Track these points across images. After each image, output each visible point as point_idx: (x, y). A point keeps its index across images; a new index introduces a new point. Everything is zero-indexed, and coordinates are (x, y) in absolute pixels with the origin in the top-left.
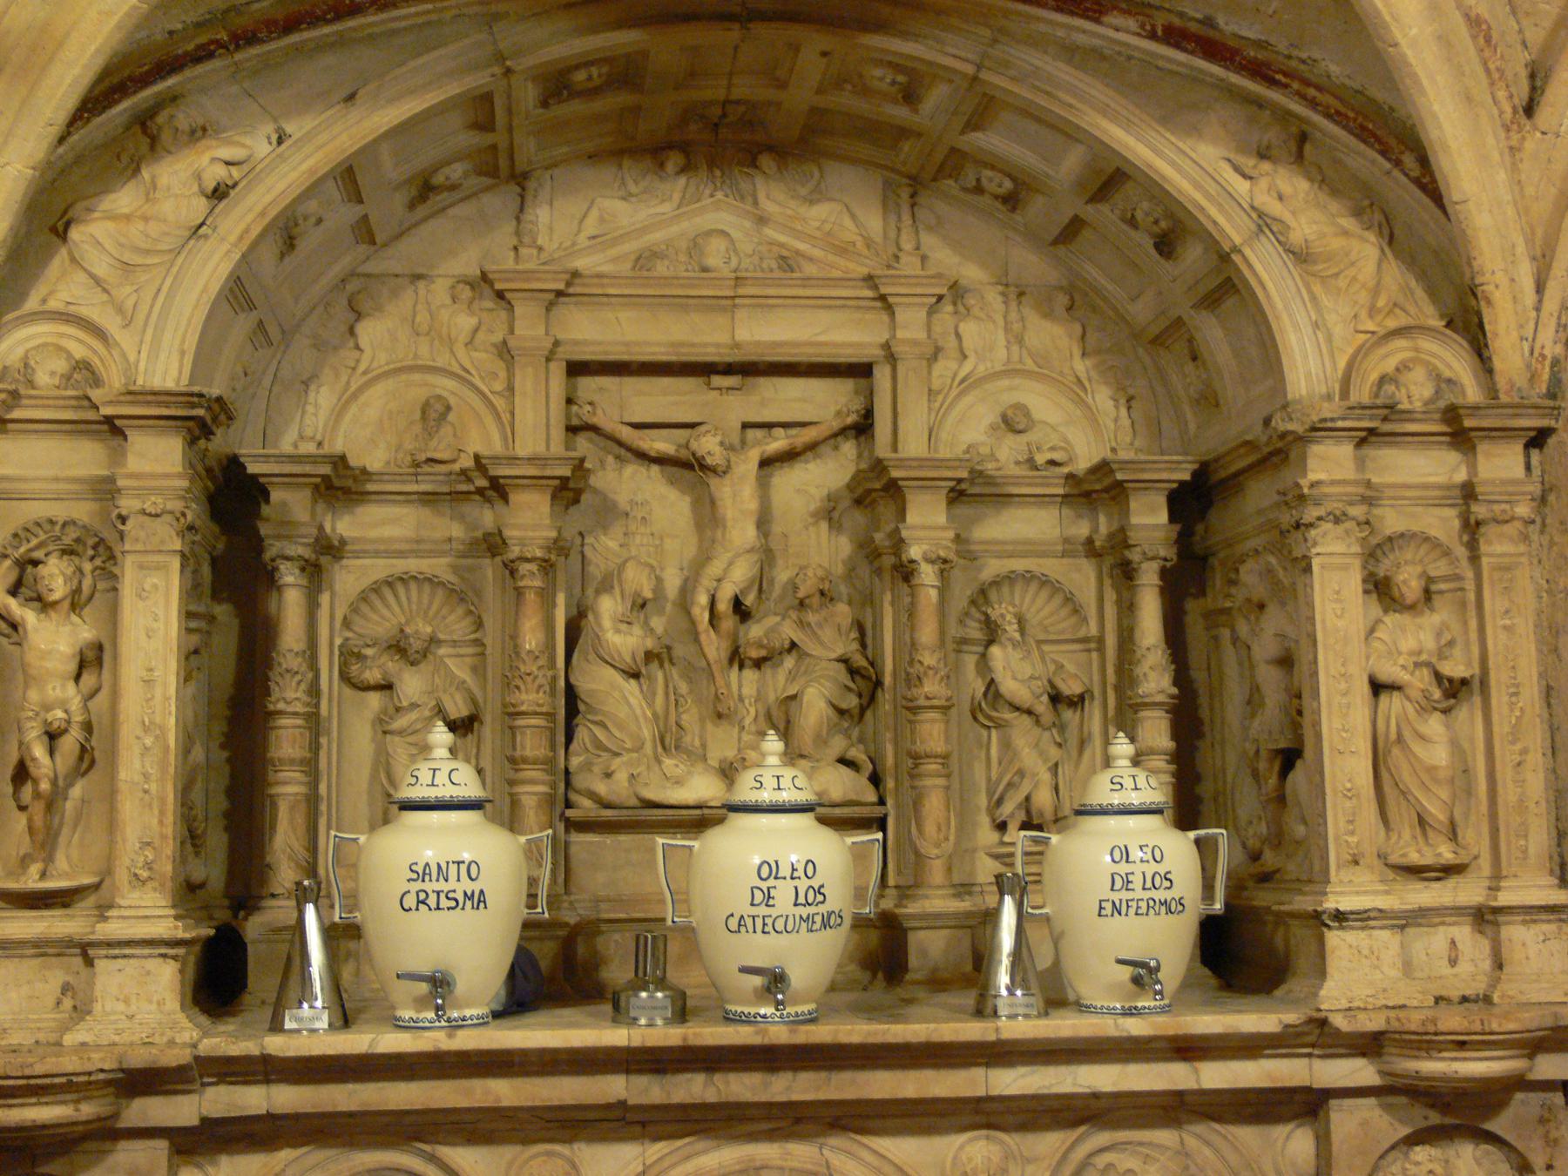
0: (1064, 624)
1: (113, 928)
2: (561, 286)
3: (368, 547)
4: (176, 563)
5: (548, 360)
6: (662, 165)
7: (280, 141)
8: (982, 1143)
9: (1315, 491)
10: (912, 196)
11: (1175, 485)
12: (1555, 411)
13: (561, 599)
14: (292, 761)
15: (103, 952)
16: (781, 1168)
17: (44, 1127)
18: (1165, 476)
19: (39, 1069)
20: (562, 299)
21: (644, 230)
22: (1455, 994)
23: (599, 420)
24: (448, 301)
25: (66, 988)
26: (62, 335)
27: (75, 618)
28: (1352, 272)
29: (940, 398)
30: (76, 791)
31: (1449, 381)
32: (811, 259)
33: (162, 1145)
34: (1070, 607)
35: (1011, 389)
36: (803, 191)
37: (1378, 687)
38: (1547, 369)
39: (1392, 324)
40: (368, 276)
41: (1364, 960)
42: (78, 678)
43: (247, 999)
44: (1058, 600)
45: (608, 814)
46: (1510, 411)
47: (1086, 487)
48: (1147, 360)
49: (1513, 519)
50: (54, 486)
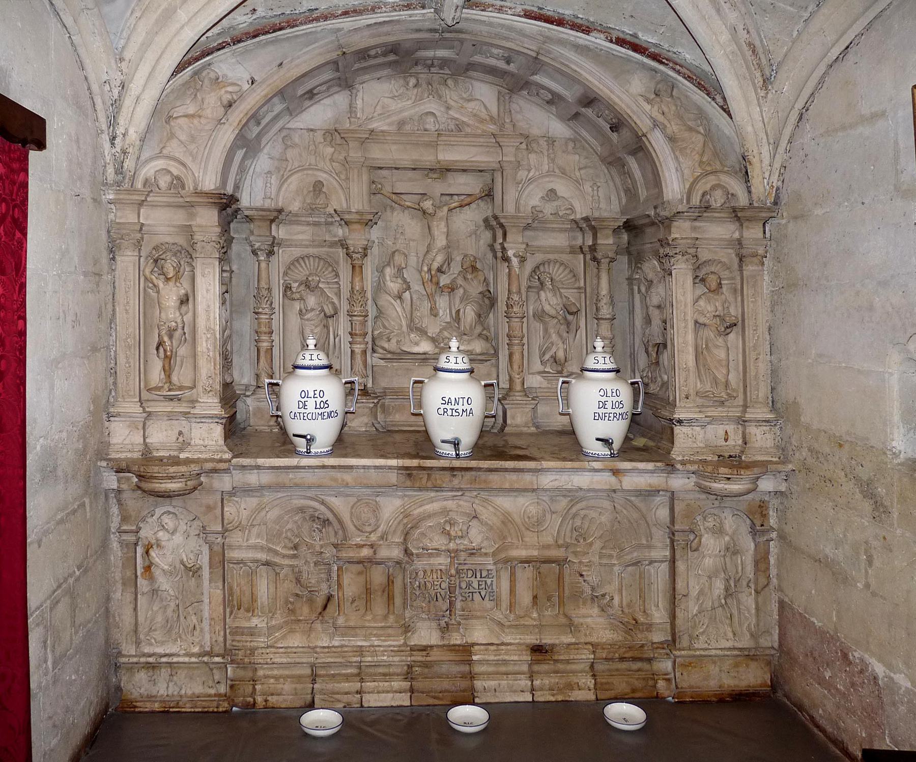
21: (401, 111)
31: (732, 195)
32: (468, 126)
34: (572, 274)
44: (567, 271)
48: (606, 171)
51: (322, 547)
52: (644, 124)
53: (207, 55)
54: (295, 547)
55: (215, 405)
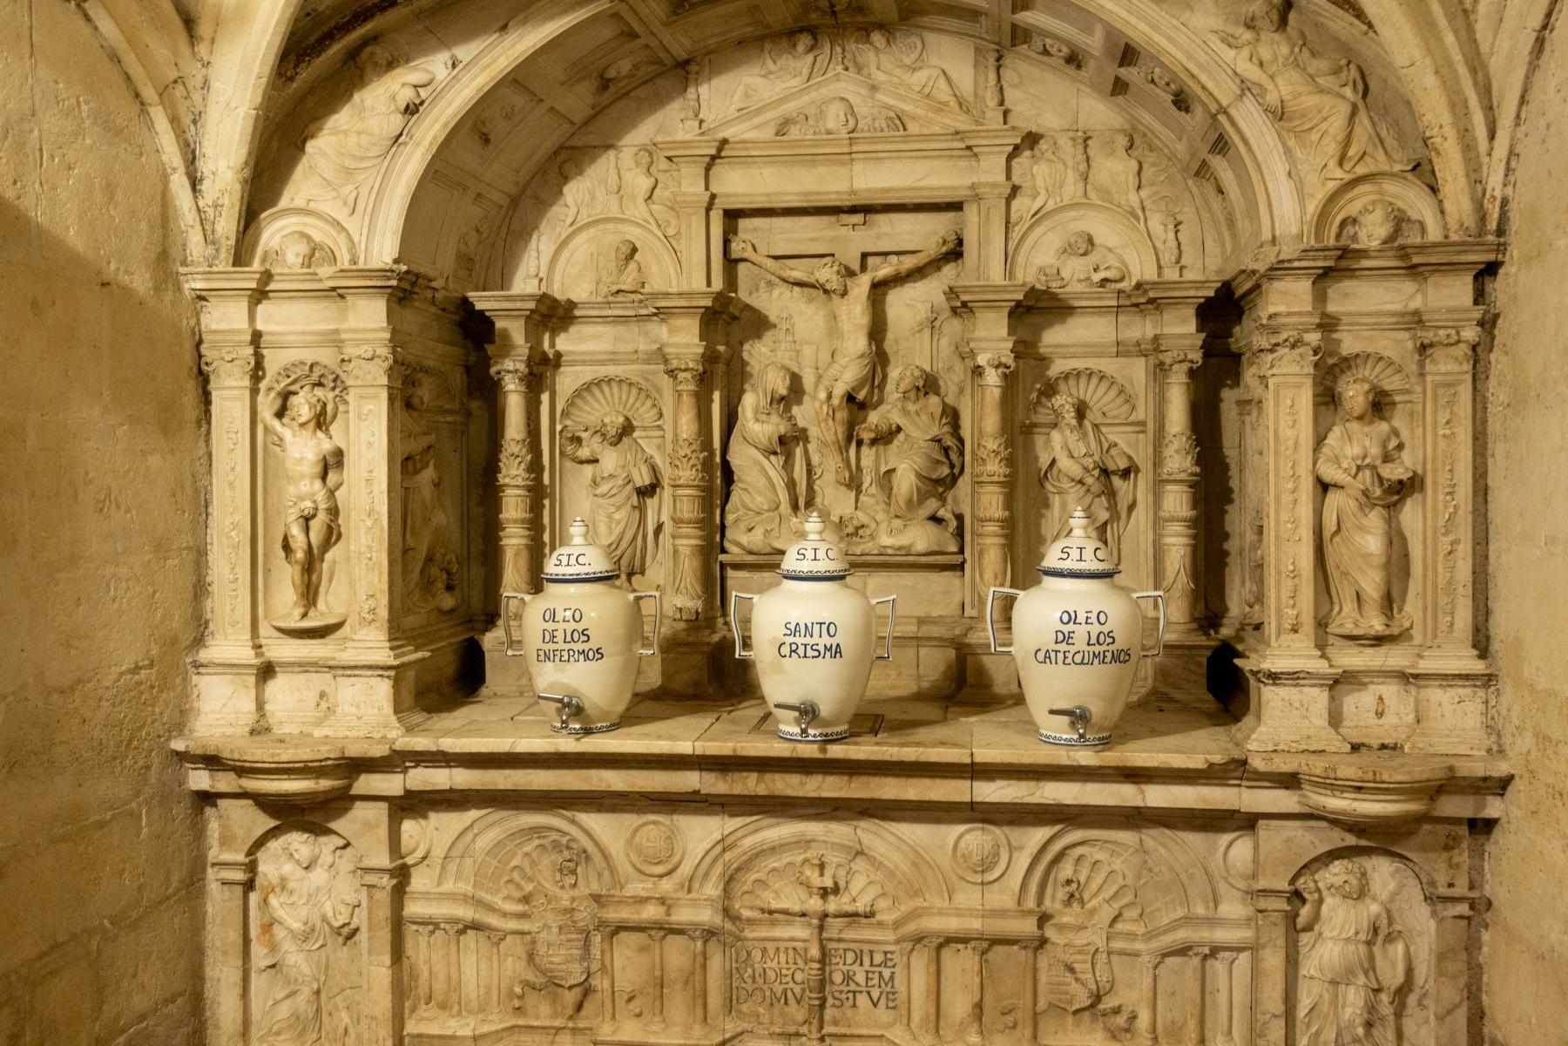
0: (1118, 410)
1: (349, 656)
2: (713, 152)
3: (578, 358)
4: (384, 395)
5: (708, 209)
6: (795, 45)
7: (454, 66)
8: (980, 833)
9: (1273, 322)
10: (998, 60)
11: (1202, 300)
12: (1501, 248)
13: (716, 396)
14: (516, 521)
15: (340, 672)
16: (826, 842)
17: (294, 794)
18: (1192, 293)
19: (284, 758)
20: (718, 161)
21: (782, 101)
22: (1375, 743)
23: (749, 254)
24: (633, 165)
25: (322, 695)
26: (305, 224)
27: (320, 434)
28: (1323, 126)
29: (1017, 228)
30: (329, 556)
33: (384, 806)
35: (1075, 219)
36: (908, 61)
37: (1324, 487)
38: (1497, 209)
39: (1361, 170)
40: (573, 148)
41: (1295, 712)
42: (324, 478)
43: (484, 691)
45: (750, 559)
46: (1460, 248)
47: (1134, 300)
48: (1194, 189)
49: (1458, 342)
50: (302, 338)
51: (573, 899)
52: (1223, 90)
53: (365, 20)
54: (526, 899)
55: (378, 645)
